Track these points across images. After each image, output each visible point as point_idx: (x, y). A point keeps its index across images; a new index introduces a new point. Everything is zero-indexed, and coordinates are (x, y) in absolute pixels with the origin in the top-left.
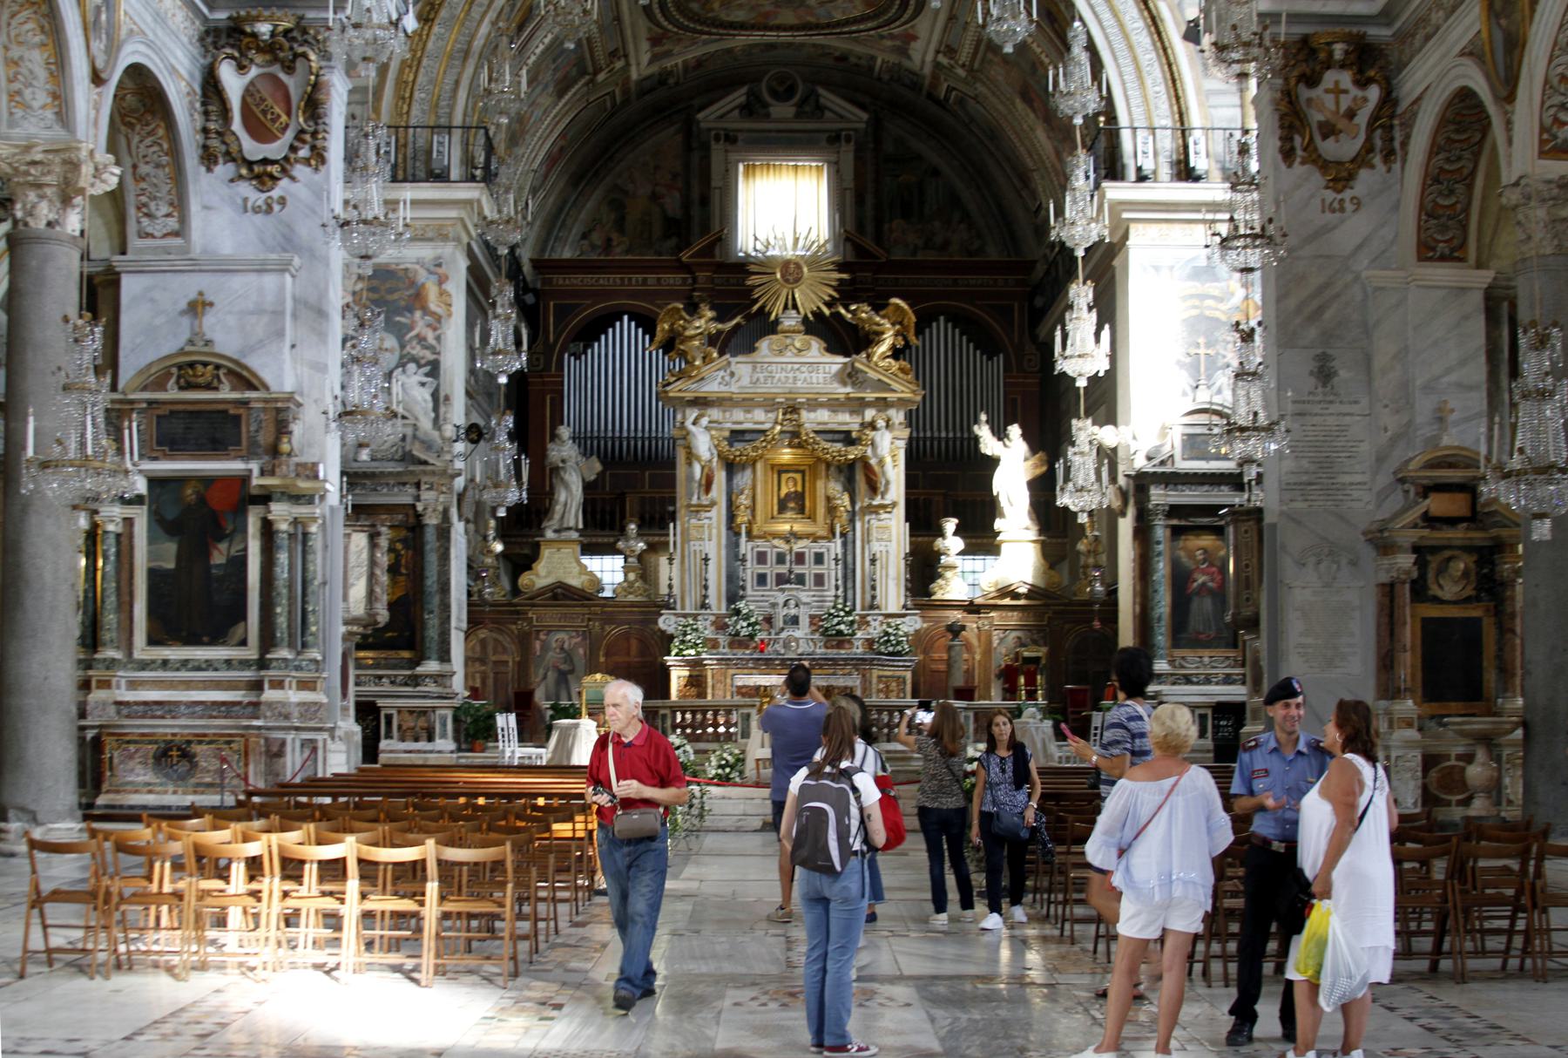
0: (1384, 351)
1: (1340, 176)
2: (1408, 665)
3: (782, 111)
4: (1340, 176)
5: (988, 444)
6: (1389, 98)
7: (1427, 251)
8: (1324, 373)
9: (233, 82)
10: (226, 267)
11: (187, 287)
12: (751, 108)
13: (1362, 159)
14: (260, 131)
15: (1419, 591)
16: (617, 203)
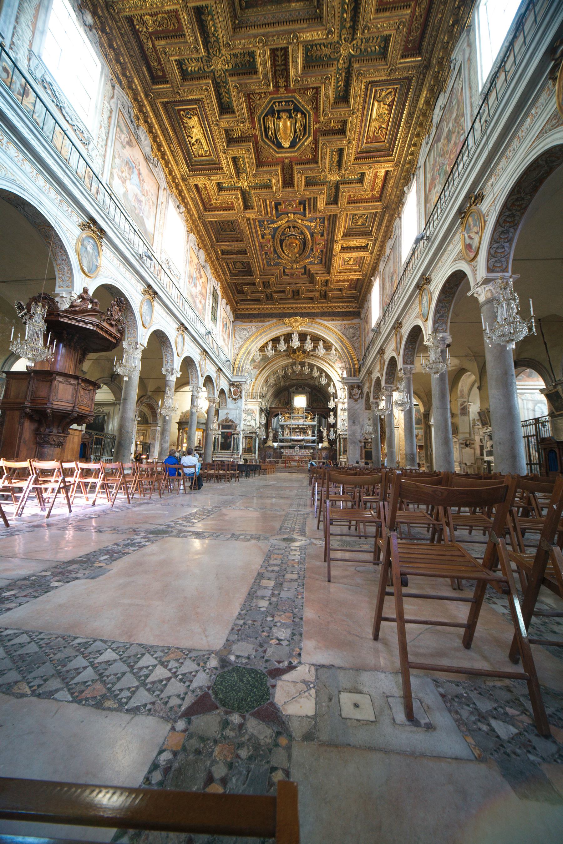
0: (361, 420)
1: (356, 400)
2: (363, 455)
3: (300, 389)
4: (356, 400)
5: (322, 430)
6: (362, 391)
7: (366, 409)
8: (354, 422)
9: (232, 390)
10: (231, 410)
11: (226, 411)
12: (297, 389)
13: (359, 398)
14: (235, 395)
15: (365, 447)
16: (280, 401)
